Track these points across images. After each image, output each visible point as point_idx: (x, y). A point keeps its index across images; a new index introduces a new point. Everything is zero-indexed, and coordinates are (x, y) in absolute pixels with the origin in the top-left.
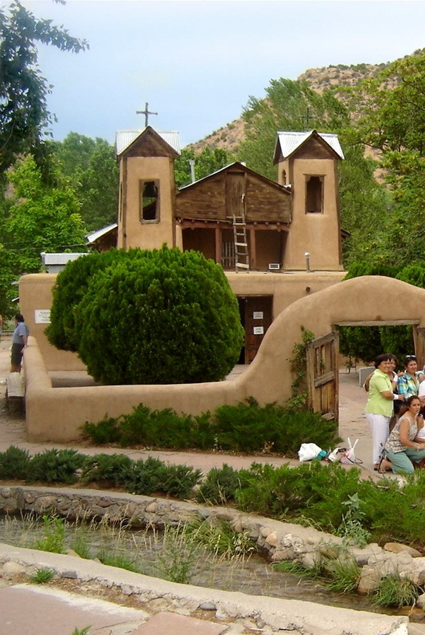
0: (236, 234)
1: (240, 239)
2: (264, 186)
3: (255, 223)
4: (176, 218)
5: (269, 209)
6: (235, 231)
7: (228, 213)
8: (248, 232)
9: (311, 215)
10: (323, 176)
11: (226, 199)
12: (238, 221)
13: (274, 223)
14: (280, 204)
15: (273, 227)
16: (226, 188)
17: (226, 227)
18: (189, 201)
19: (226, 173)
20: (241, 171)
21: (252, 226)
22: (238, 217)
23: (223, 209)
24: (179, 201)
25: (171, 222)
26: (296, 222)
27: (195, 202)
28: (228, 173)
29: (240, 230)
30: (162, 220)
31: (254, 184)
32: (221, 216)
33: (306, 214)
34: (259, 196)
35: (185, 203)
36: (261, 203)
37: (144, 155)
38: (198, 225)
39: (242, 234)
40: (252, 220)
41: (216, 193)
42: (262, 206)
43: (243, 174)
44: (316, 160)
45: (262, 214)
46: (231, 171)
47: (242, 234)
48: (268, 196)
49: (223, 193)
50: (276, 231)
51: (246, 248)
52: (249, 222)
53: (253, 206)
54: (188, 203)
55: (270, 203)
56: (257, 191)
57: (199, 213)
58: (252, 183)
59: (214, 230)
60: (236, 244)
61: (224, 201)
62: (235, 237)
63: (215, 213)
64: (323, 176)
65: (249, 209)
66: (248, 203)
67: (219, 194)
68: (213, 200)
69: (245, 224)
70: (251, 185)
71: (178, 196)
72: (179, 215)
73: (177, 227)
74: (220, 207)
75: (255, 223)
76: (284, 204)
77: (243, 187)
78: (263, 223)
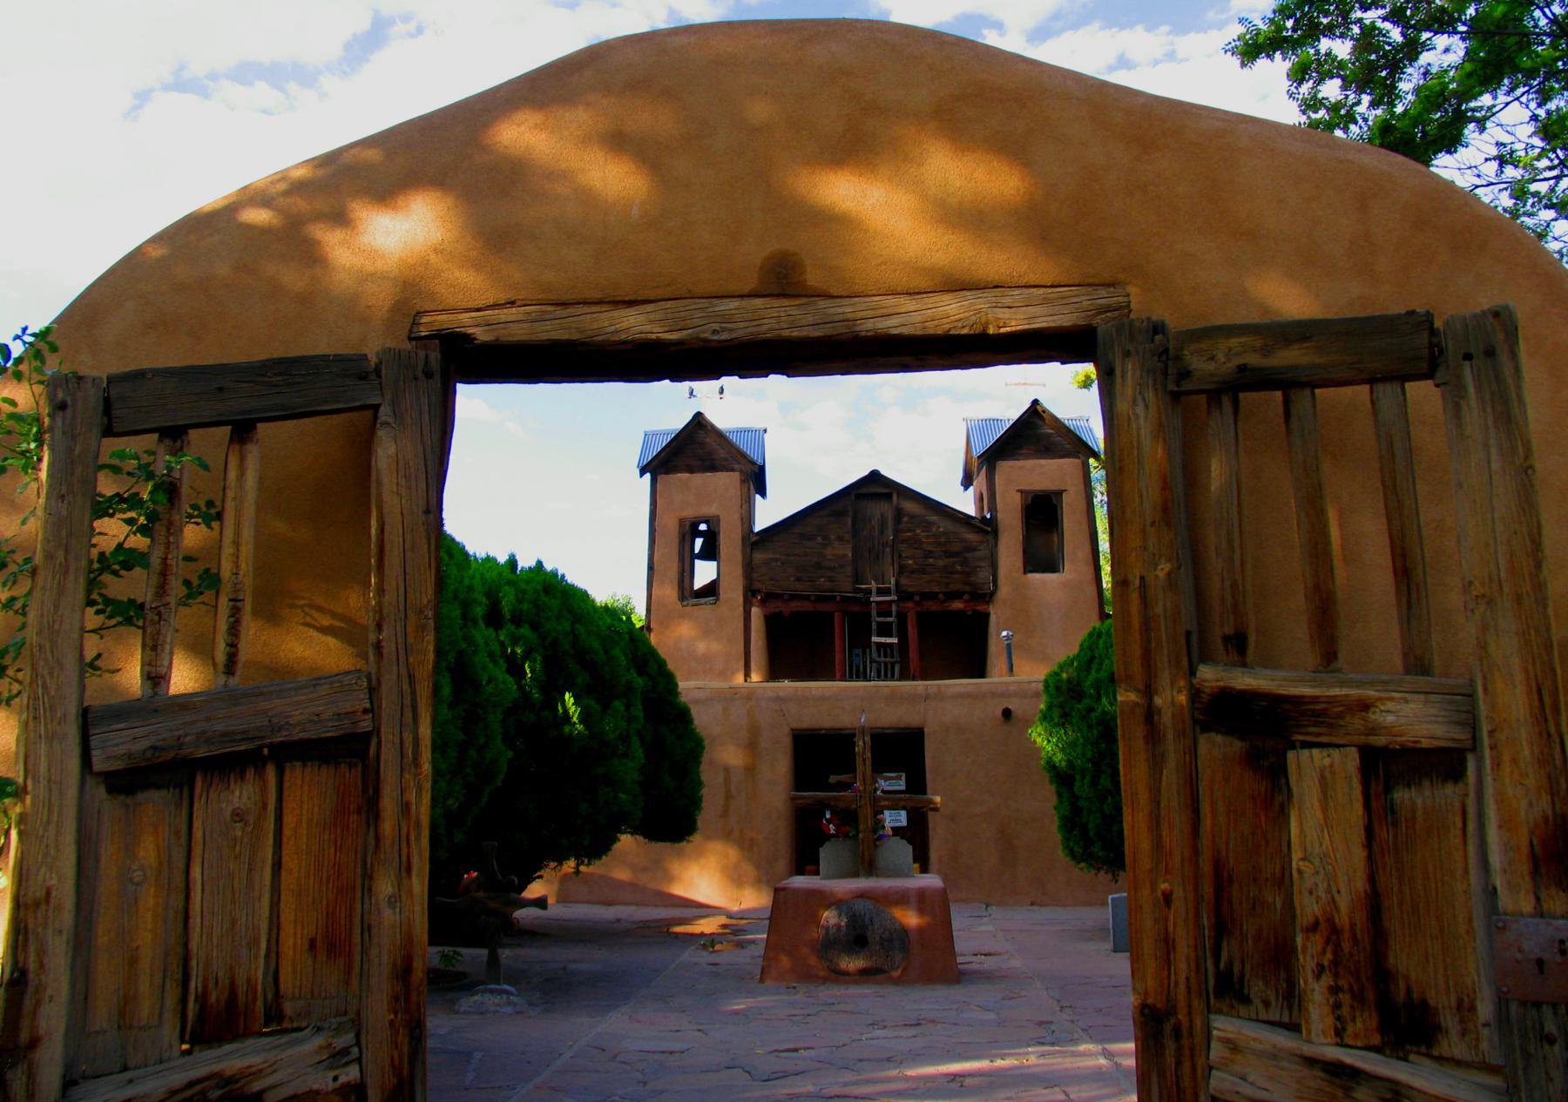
0: (876, 619)
1: (884, 630)
2: (933, 518)
3: (917, 598)
4: (750, 593)
5: (946, 567)
6: (874, 613)
7: (858, 577)
8: (902, 617)
9: (1036, 577)
10: (1059, 493)
11: (854, 551)
12: (880, 592)
13: (956, 595)
14: (969, 555)
15: (957, 605)
16: (854, 525)
17: (856, 608)
18: (778, 556)
19: (853, 496)
20: (886, 491)
21: (910, 605)
22: (881, 588)
23: (849, 570)
24: (759, 556)
25: (741, 600)
26: (1004, 591)
27: (792, 558)
28: (858, 497)
29: (884, 609)
30: (722, 596)
31: (912, 517)
32: (845, 585)
33: (1025, 573)
34: (924, 540)
35: (772, 559)
36: (929, 554)
37: (691, 471)
38: (795, 606)
39: (889, 619)
40: (911, 590)
41: (832, 537)
42: (931, 560)
43: (888, 496)
44: (1043, 462)
45: (927, 577)
46: (863, 491)
47: (889, 619)
48: (942, 540)
49: (847, 537)
50: (960, 612)
51: (895, 647)
52: (904, 595)
53: (910, 562)
54: (776, 560)
55: (948, 554)
56: (918, 531)
57: (798, 579)
58: (908, 515)
59: (831, 615)
60: (875, 639)
61: (850, 555)
62: (874, 626)
63: (831, 580)
64: (1059, 493)
65: (902, 570)
66: (900, 556)
67: (841, 539)
68: (829, 552)
69: (896, 598)
70: (905, 519)
71: (754, 545)
72: (757, 585)
73: (754, 610)
74: (842, 566)
75: (917, 598)
76: (977, 554)
77: (890, 523)
78: (932, 596)
